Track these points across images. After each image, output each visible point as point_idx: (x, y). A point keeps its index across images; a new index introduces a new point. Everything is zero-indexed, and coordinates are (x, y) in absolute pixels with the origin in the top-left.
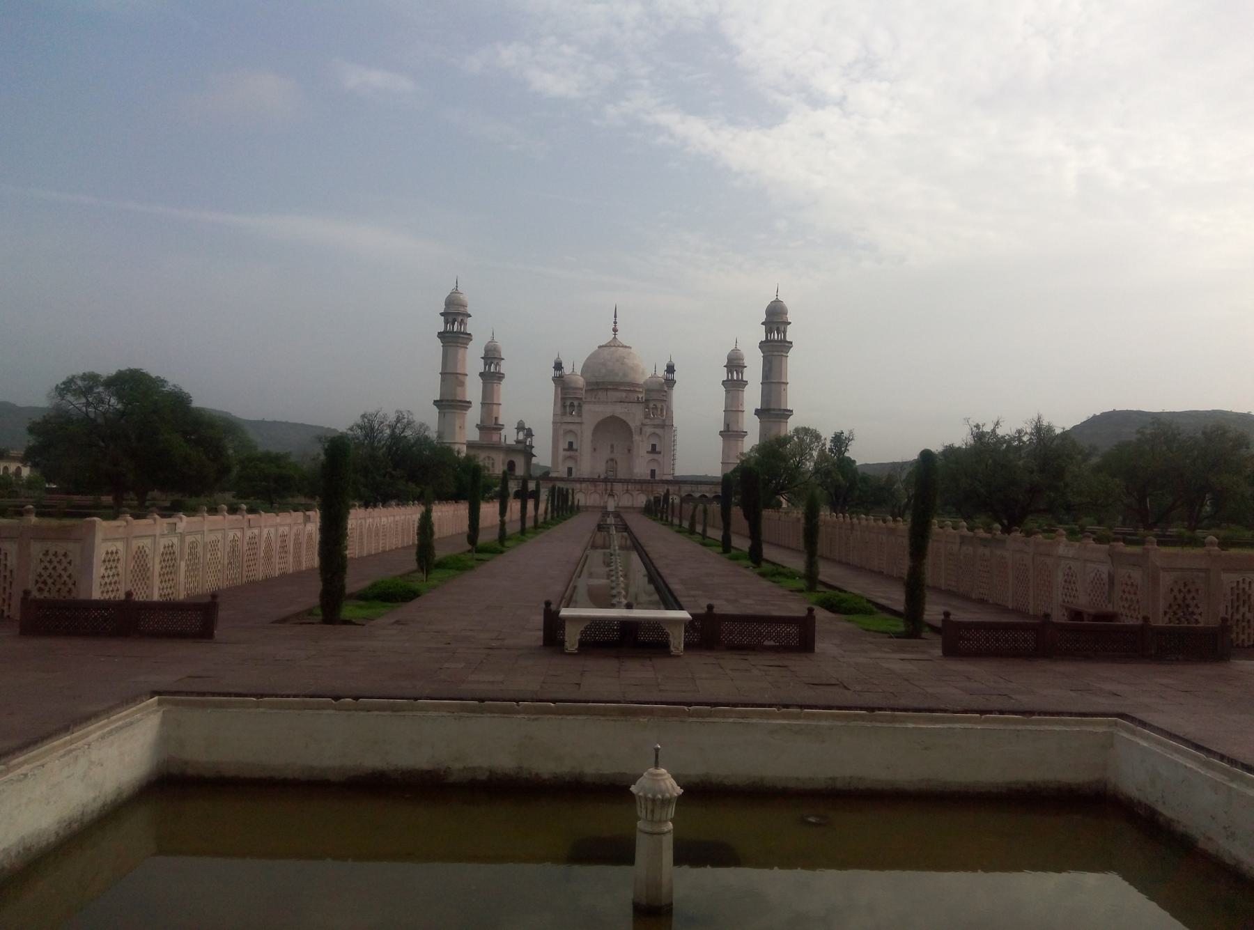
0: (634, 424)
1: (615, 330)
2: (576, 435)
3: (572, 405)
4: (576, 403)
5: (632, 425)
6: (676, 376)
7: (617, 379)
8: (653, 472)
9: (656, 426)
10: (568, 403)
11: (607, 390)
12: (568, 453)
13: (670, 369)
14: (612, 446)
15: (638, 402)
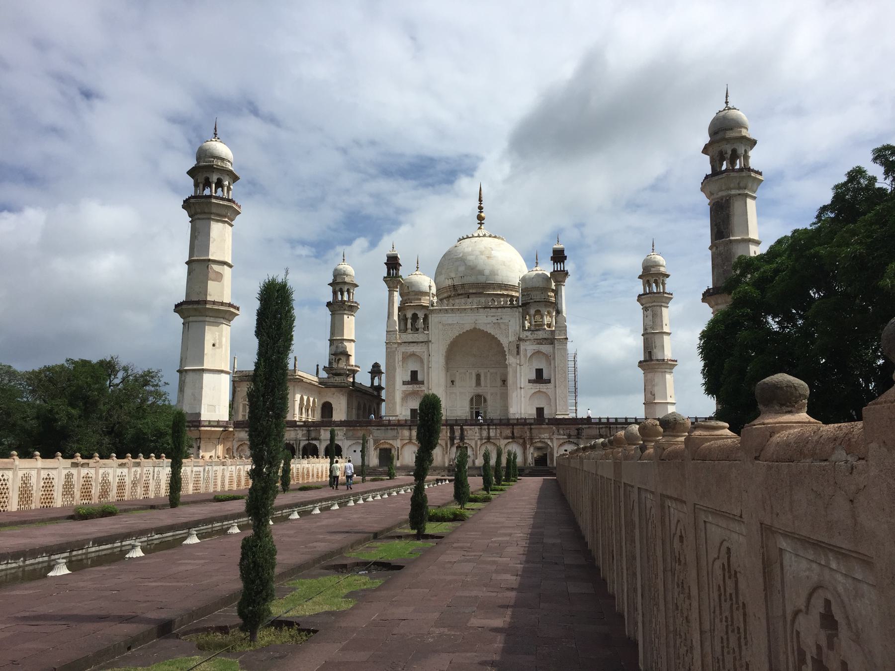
0: (506, 341)
1: (480, 218)
2: (422, 361)
3: (415, 317)
4: (421, 315)
5: (504, 341)
6: (569, 266)
7: (482, 279)
8: (540, 411)
9: (541, 341)
10: (409, 315)
11: (468, 296)
12: (410, 388)
13: (559, 256)
14: (478, 376)
15: (512, 307)
